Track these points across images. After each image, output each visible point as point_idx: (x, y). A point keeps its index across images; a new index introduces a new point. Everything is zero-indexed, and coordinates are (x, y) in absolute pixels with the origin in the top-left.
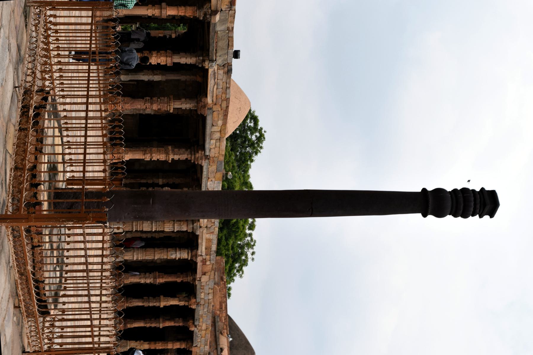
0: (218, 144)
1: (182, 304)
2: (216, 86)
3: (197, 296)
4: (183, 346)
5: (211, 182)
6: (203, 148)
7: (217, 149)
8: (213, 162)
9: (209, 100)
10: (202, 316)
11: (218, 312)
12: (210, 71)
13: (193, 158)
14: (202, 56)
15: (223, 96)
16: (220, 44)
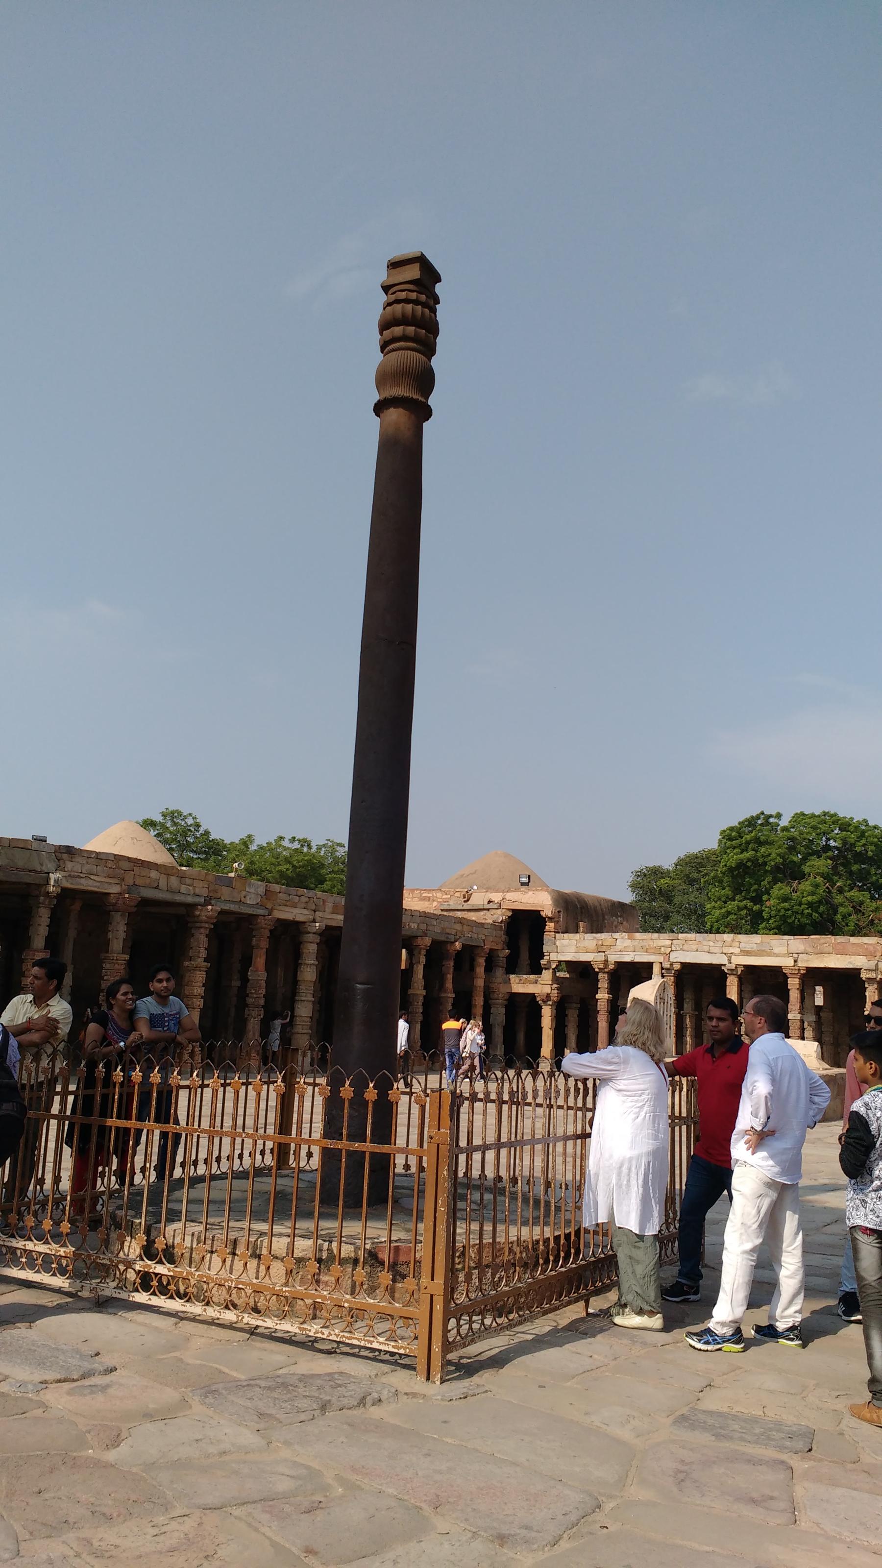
0: (188, 881)
1: (423, 959)
2: (92, 877)
3: (414, 934)
4: (482, 961)
5: (248, 898)
6: (193, 906)
7: (196, 883)
8: (216, 891)
9: (114, 889)
10: (443, 929)
11: (435, 904)
12: (67, 884)
13: (207, 926)
14: (38, 896)
15: (109, 866)
16: (20, 864)
